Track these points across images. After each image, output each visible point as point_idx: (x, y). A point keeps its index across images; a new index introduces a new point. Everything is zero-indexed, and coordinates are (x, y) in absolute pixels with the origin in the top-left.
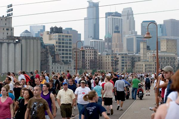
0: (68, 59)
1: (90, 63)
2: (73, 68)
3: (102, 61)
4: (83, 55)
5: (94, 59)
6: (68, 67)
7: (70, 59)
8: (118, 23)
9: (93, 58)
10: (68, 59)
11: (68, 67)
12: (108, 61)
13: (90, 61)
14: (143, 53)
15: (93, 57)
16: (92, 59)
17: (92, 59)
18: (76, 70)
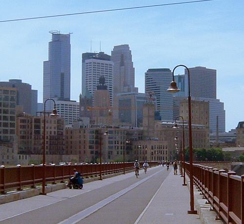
0: (9, 135)
1: (49, 143)
2: (16, 151)
3: (71, 138)
4: (37, 127)
5: (56, 135)
6: (8, 150)
7: (12, 135)
8: (64, 111)
9: (55, 132)
10: (9, 135)
11: (8, 150)
12: (82, 139)
13: (50, 139)
14: (147, 125)
15: (56, 130)
16: (53, 134)
17: (53, 134)
18: (21, 155)
